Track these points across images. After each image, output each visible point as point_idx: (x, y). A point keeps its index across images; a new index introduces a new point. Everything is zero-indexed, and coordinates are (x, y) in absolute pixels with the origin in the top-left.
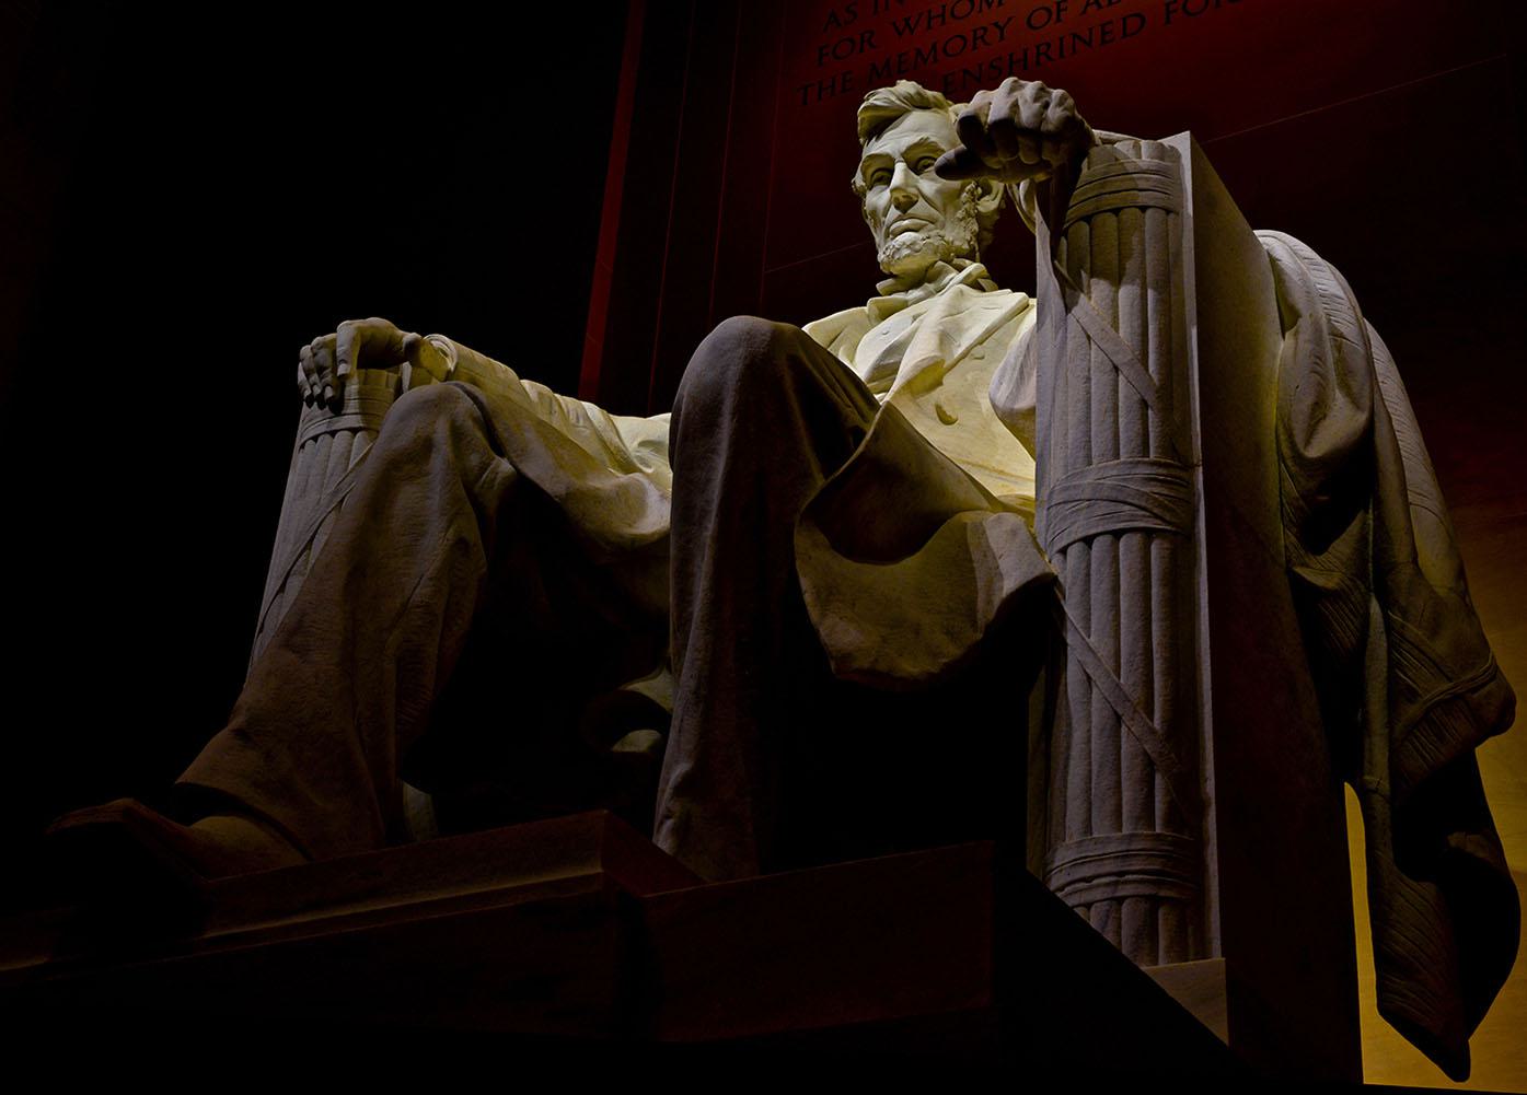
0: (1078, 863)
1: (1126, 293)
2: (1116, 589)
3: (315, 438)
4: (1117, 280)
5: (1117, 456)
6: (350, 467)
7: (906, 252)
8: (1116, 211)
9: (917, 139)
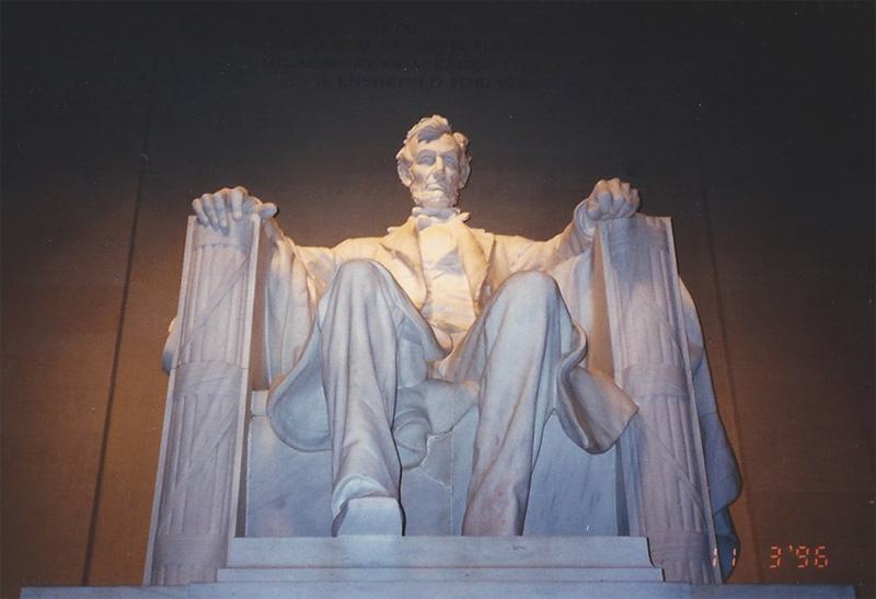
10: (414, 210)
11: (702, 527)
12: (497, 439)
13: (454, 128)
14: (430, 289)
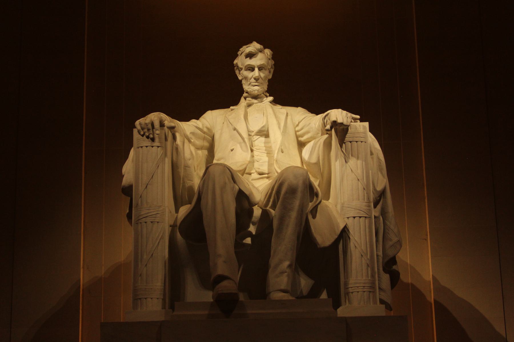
0: (355, 283)
1: (359, 162)
2: (360, 229)
3: (147, 147)
4: (358, 158)
5: (359, 200)
6: (159, 157)
7: (256, 92)
8: (357, 142)
9: (262, 63)
10: (245, 95)
13: (265, 48)
14: (253, 148)
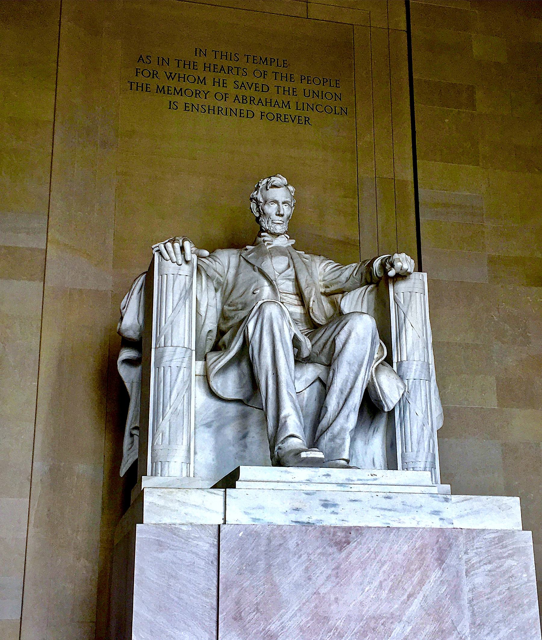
10: (262, 234)
11: (433, 451)
12: (338, 403)
